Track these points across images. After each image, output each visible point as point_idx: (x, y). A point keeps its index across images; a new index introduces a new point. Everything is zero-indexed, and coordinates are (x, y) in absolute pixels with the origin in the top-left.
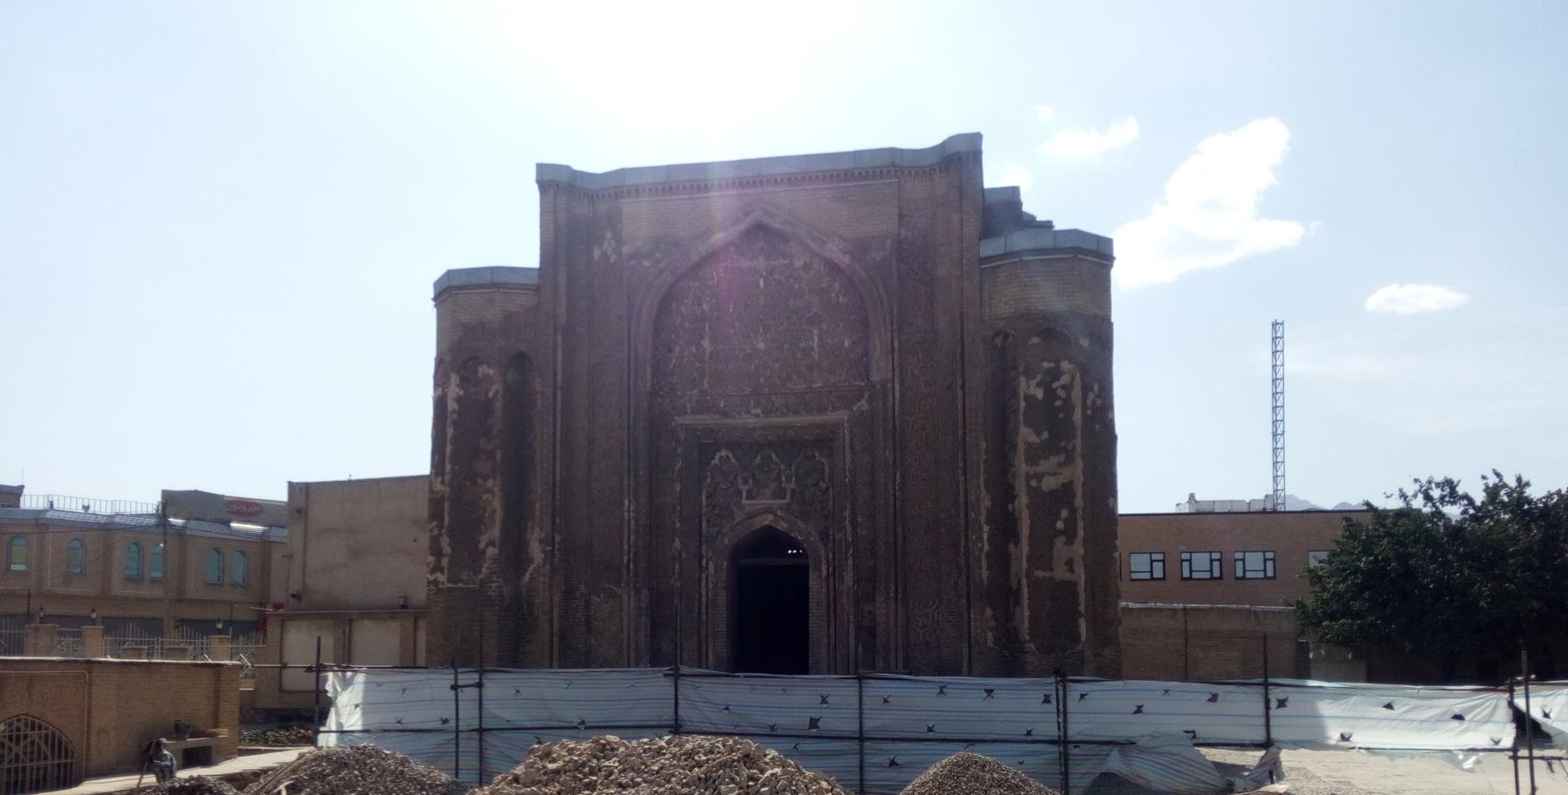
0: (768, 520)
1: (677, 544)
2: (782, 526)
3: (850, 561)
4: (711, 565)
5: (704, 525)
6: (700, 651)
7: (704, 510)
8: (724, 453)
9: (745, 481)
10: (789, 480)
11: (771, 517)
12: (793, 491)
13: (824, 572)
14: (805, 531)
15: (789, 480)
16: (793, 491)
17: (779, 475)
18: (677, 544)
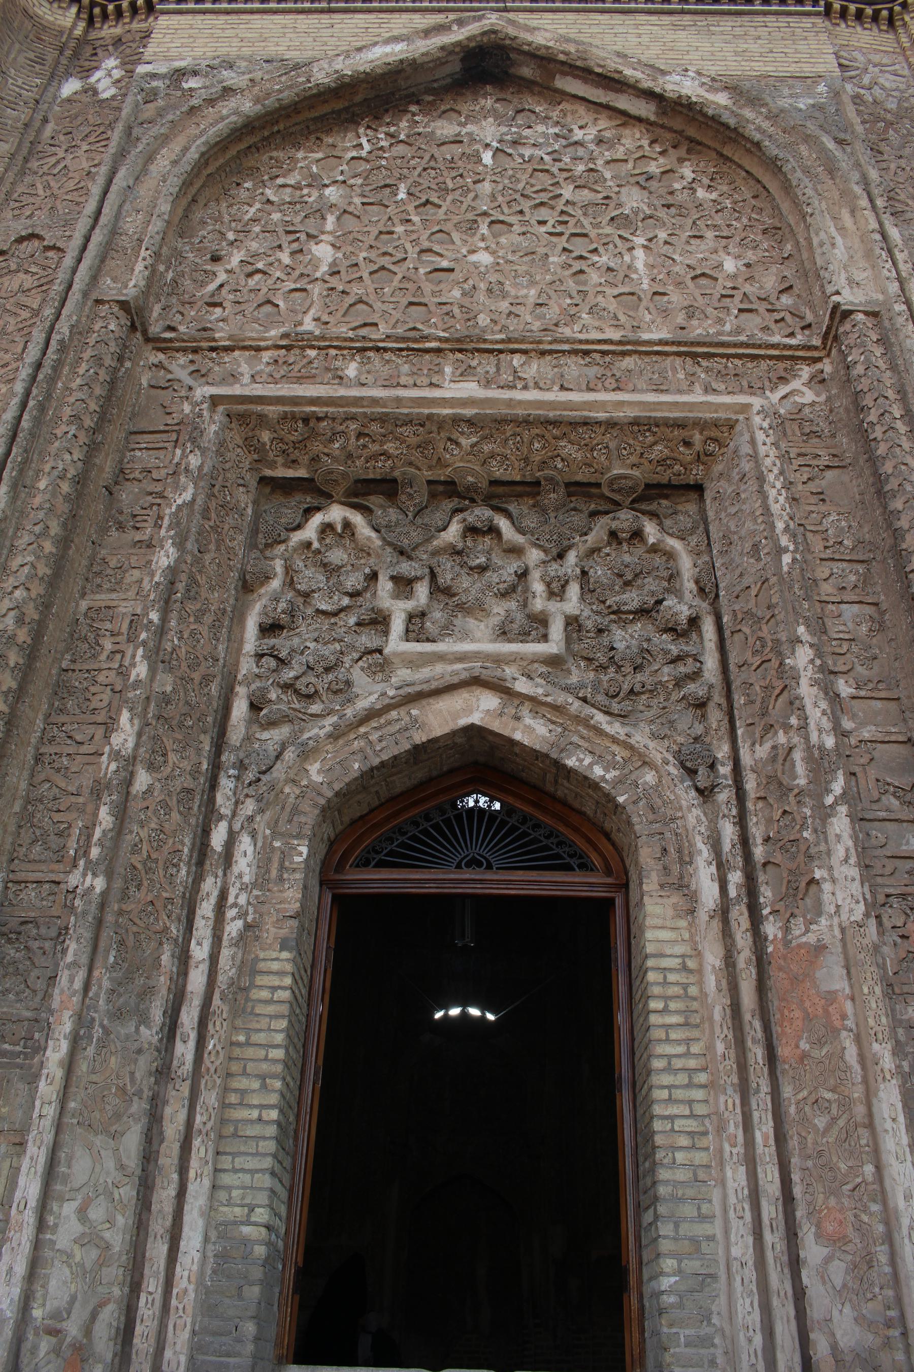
0: (480, 709)
1: (125, 734)
2: (532, 732)
3: (840, 824)
4: (245, 843)
5: (240, 709)
6: (144, 1203)
7: (247, 666)
8: (336, 513)
9: (403, 585)
10: (556, 592)
11: (489, 701)
12: (572, 623)
13: (709, 893)
14: (620, 756)
15: (556, 592)
16: (572, 623)
17: (523, 575)
18: (125, 734)
